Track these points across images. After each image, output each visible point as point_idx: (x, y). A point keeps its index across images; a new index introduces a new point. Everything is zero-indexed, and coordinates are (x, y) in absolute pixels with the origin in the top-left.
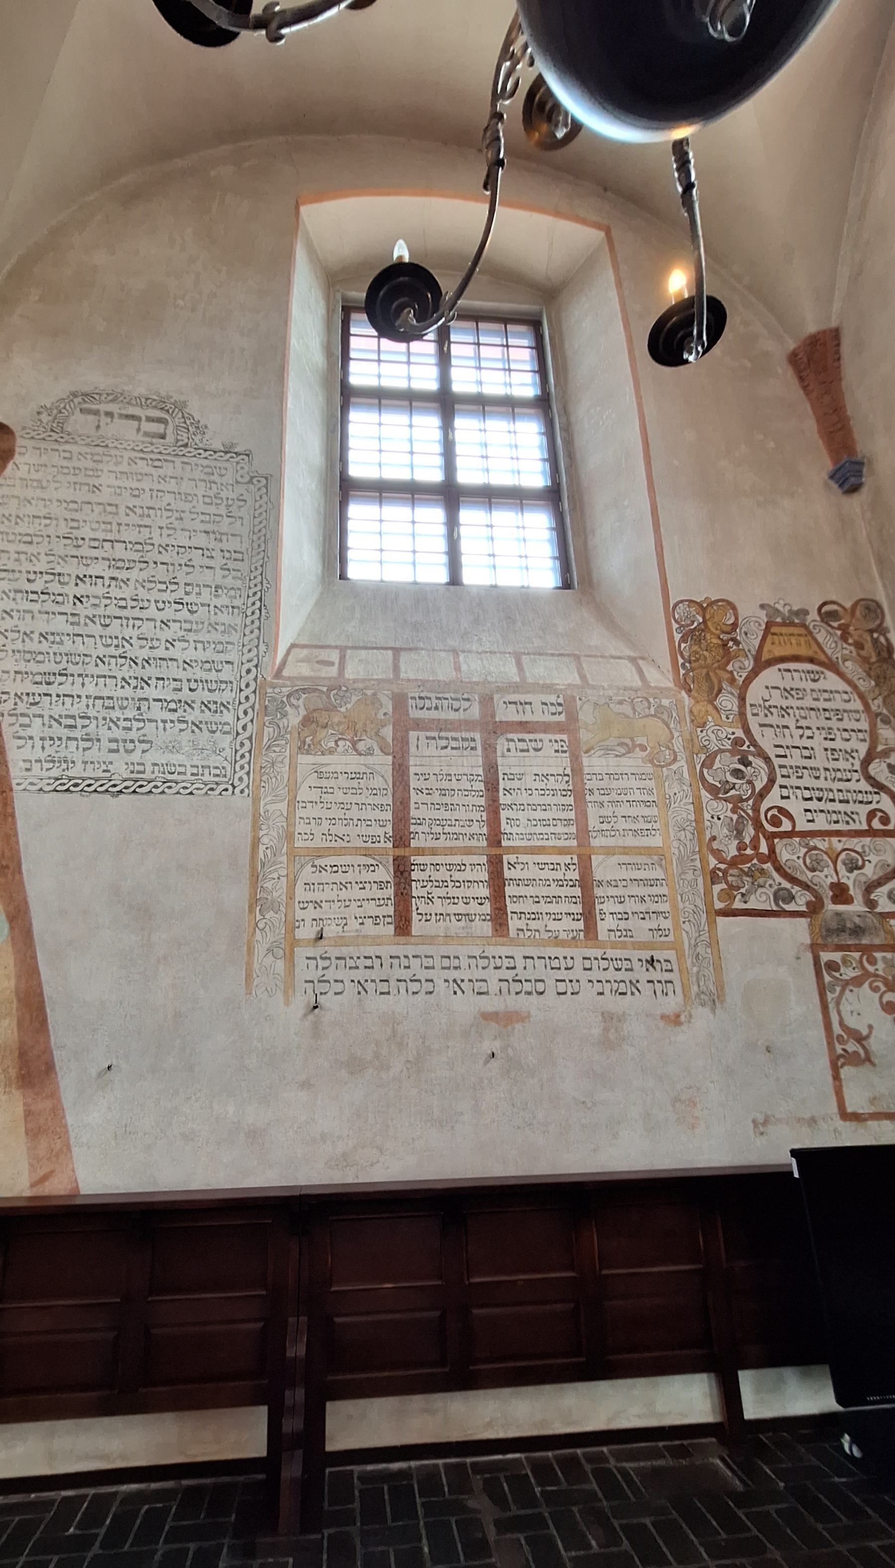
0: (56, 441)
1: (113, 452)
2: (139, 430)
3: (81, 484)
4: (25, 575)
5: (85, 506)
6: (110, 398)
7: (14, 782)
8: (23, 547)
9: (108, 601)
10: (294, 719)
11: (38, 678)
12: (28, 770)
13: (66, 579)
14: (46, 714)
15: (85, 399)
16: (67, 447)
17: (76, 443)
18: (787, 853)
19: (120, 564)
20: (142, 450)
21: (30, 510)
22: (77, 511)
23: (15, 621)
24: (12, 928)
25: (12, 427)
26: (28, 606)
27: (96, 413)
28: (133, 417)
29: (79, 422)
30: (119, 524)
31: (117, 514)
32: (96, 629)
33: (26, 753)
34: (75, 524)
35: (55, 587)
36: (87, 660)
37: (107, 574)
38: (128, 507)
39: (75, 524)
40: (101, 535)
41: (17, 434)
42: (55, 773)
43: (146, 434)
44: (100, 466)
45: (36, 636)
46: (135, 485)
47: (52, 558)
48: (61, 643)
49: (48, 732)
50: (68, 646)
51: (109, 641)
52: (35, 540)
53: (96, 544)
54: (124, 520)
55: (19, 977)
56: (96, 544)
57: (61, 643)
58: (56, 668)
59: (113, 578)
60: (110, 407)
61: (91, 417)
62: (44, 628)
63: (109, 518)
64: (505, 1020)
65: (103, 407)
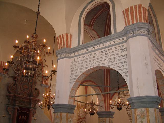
18: (80, 120)
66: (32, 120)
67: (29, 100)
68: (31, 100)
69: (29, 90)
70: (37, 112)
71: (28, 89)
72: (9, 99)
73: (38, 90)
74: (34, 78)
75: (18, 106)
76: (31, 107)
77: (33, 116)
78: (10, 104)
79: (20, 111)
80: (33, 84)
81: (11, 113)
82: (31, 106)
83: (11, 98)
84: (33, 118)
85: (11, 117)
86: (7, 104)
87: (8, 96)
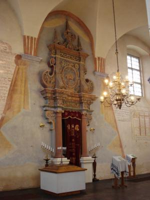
10: (132, 114)
64: (146, 142)
66: (87, 131)
67: (78, 99)
68: (82, 99)
69: (76, 81)
70: (93, 118)
71: (74, 80)
72: (45, 98)
73: (91, 81)
74: (81, 62)
75: (62, 108)
77: (88, 125)
78: (48, 106)
80: (82, 72)
81: (51, 121)
82: (84, 108)
83: (49, 95)
84: (88, 129)
85: (54, 128)
86: (44, 107)
87: (43, 93)
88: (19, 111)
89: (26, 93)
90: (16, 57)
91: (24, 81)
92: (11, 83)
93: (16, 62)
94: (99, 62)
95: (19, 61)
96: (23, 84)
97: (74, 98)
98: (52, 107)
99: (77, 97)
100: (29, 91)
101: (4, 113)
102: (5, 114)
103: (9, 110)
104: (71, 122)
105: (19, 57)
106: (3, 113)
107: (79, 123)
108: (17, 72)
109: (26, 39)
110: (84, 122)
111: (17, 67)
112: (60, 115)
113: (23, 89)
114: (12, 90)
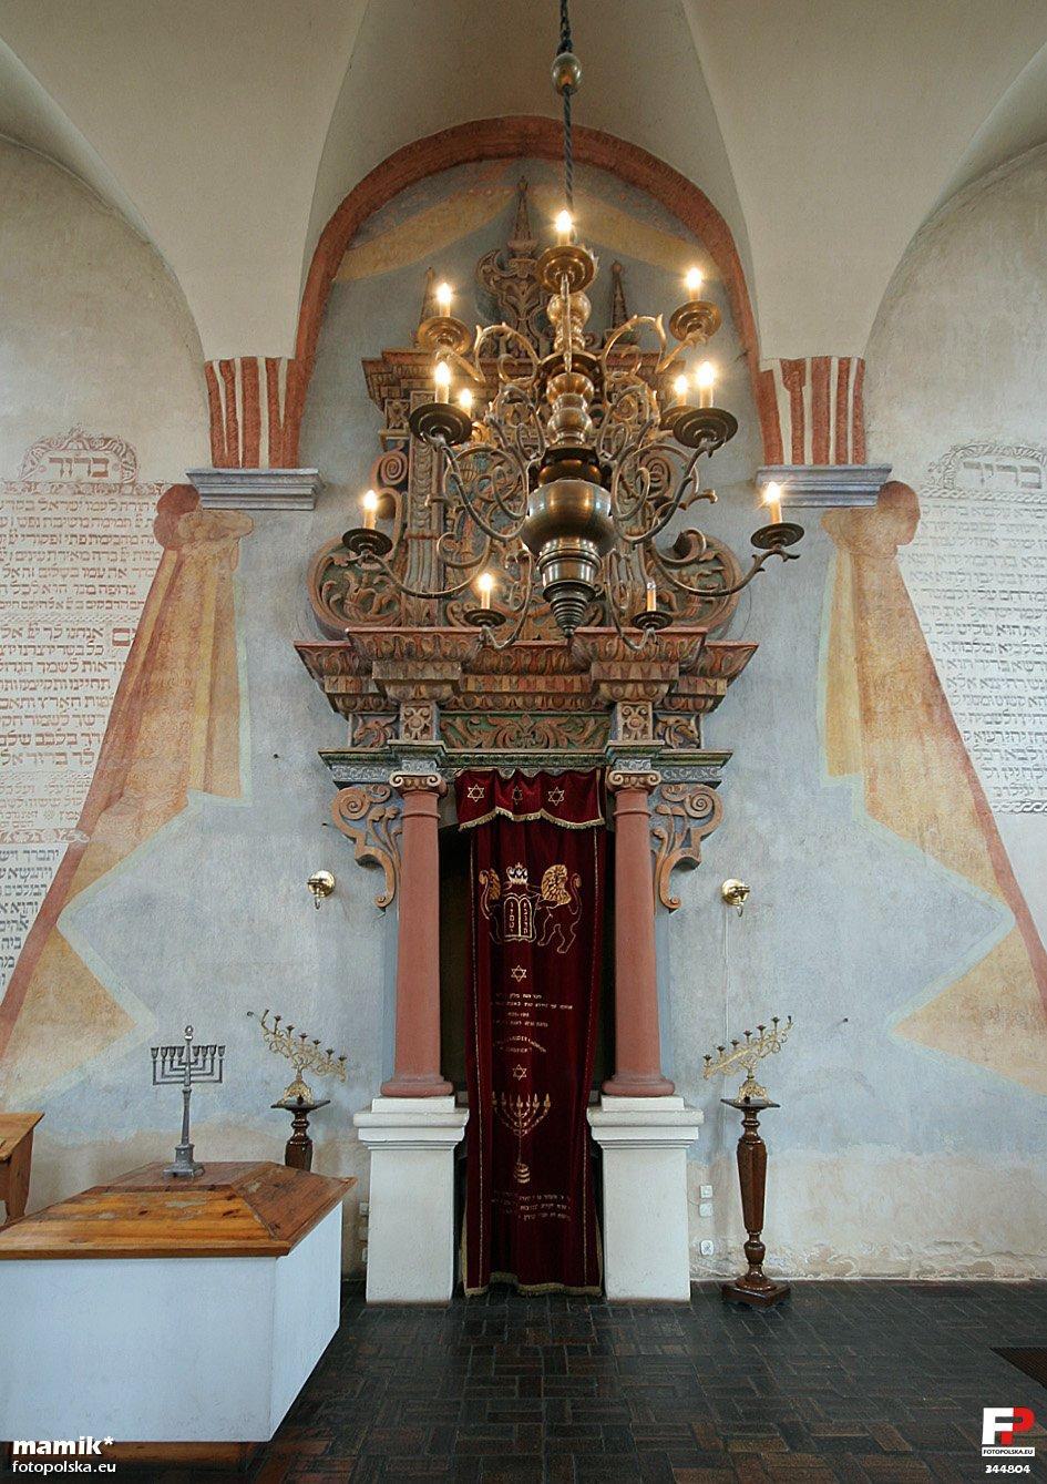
0: (950, 497)
1: (1001, 505)
2: (1017, 481)
3: (982, 539)
4: (957, 628)
5: (989, 561)
6: (986, 450)
7: (991, 805)
8: (949, 603)
9: (1027, 649)
11: (989, 719)
12: (999, 795)
13: (990, 630)
14: (1002, 748)
15: (964, 452)
16: (962, 503)
17: (968, 498)
19: (1029, 614)
20: (1024, 502)
21: (946, 567)
22: (982, 565)
23: (959, 670)
24: (1017, 918)
25: (911, 487)
26: (966, 656)
27: (978, 466)
28: (1008, 468)
29: (966, 478)
30: (1020, 576)
31: (1015, 566)
32: (1022, 674)
33: (994, 782)
34: (984, 578)
35: (982, 638)
36: (1023, 701)
37: (1022, 623)
38: (1023, 559)
39: (984, 578)
40: (1009, 588)
41: (918, 493)
42: (1020, 797)
43: (1024, 485)
44: (992, 520)
45: (977, 682)
46: (1026, 537)
47: (975, 611)
48: (998, 687)
49: (1007, 764)
50: (1004, 690)
51: (1036, 684)
52: (957, 595)
53: (1005, 596)
54: (1023, 571)
55: (1030, 953)
56: (1005, 596)
57: (998, 687)
58: (999, 710)
59: (1027, 627)
60: (984, 460)
61: (975, 472)
62: (981, 675)
63: (1010, 571)
65: (984, 460)
67: (576, 682)
76: (622, 752)
77: (687, 865)
79: (487, 805)
88: (178, 806)
89: (222, 698)
90: (160, 506)
91: (207, 633)
92: (132, 655)
93: (165, 534)
94: (797, 402)
95: (182, 526)
96: (206, 651)
97: (541, 684)
98: (374, 761)
99: (555, 672)
100: (243, 685)
101: (86, 823)
102: (89, 833)
103: (116, 807)
104: (499, 845)
105: (179, 499)
106: (78, 828)
107: (595, 861)
108: (169, 588)
109: (229, 384)
110: (640, 838)
111: (173, 556)
112: (430, 804)
113: (204, 677)
114: (136, 693)
